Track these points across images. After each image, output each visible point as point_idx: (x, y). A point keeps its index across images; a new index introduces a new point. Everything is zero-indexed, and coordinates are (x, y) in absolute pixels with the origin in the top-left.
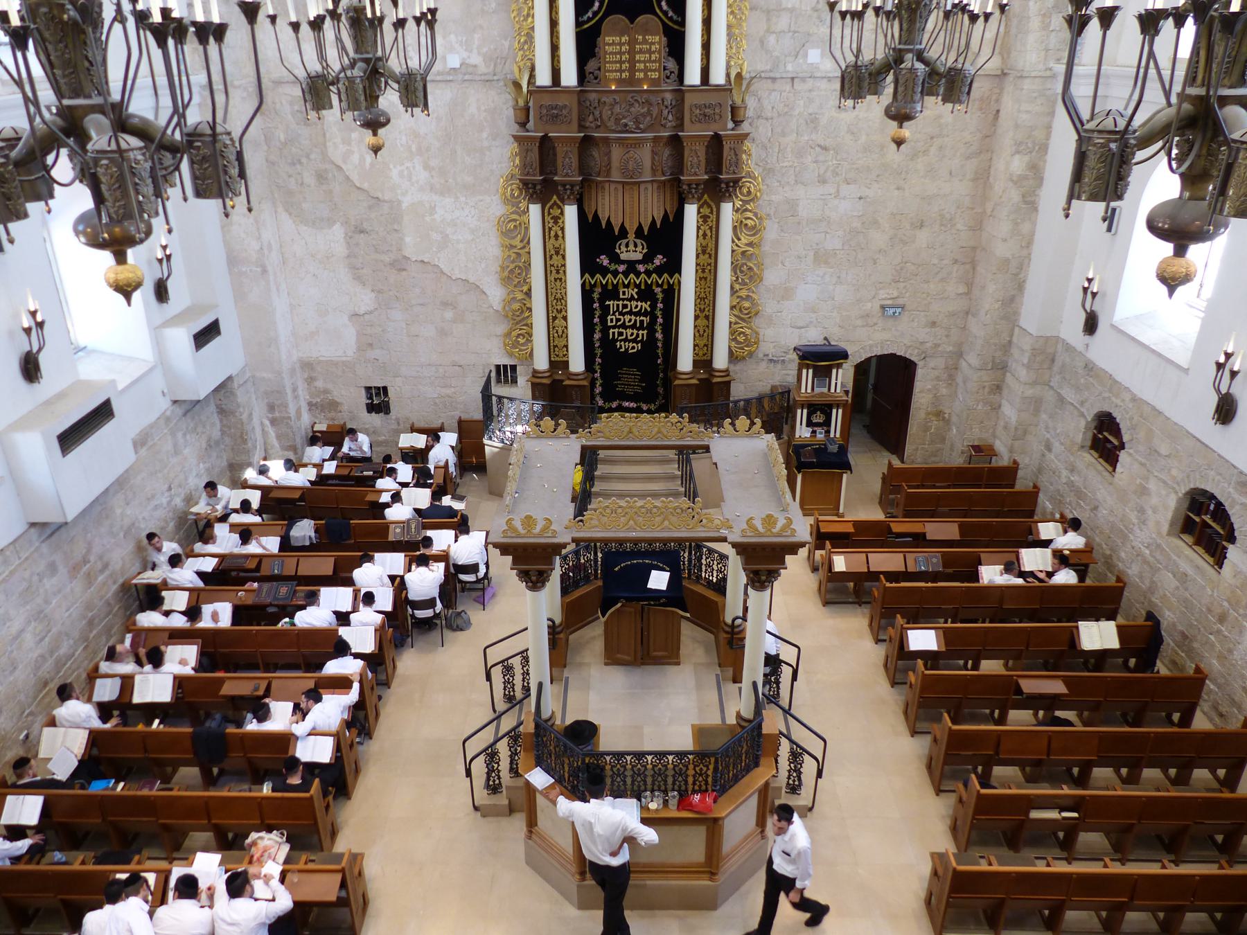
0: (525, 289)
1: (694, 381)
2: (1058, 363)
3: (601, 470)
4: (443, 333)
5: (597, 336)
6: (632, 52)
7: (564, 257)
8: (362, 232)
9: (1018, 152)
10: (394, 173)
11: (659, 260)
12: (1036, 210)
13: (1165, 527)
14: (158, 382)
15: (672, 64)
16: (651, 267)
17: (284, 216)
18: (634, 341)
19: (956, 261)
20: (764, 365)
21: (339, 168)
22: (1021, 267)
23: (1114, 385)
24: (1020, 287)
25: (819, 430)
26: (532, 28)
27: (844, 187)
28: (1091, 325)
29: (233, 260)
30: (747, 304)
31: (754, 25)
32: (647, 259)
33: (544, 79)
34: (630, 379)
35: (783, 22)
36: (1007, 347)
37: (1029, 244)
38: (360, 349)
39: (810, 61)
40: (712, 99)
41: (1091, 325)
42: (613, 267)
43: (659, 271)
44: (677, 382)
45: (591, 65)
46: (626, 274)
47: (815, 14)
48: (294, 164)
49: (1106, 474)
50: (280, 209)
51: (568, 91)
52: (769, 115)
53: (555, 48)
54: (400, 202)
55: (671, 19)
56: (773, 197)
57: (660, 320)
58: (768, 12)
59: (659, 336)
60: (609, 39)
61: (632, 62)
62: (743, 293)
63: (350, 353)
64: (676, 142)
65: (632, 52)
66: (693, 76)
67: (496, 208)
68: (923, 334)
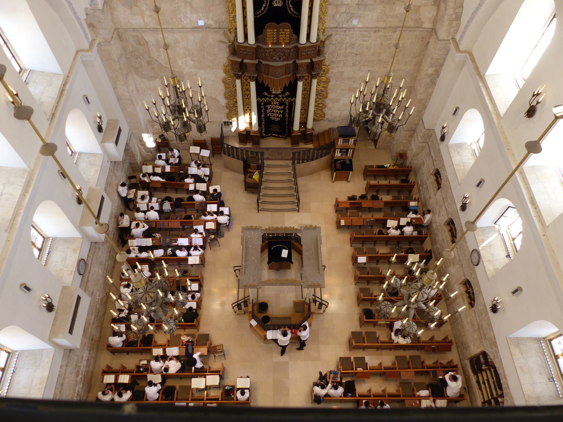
0: (235, 100)
1: (300, 134)
3: (266, 170)
5: (263, 116)
6: (278, 35)
7: (250, 91)
9: (431, 67)
10: (180, 62)
11: (287, 94)
12: (435, 84)
13: (443, 223)
14: (106, 158)
15: (295, 36)
16: (284, 96)
17: (135, 76)
18: (277, 117)
20: (326, 122)
21: (156, 60)
22: (426, 102)
23: (443, 165)
24: (425, 108)
25: (344, 154)
26: (235, 16)
29: (119, 99)
30: (321, 105)
31: (331, 10)
32: (282, 93)
33: (241, 39)
34: (276, 128)
35: (343, 9)
36: (417, 124)
39: (353, 23)
41: (443, 138)
42: (269, 96)
43: (287, 97)
44: (293, 134)
45: (261, 36)
46: (274, 98)
47: (357, 6)
48: (137, 58)
49: (435, 189)
50: (134, 74)
52: (334, 42)
53: (245, 26)
54: (182, 72)
55: (295, 14)
56: (334, 71)
57: (287, 111)
58: (337, 6)
59: (287, 115)
60: (269, 30)
62: (320, 102)
64: (295, 65)
65: (278, 35)
66: (303, 39)
67: (222, 75)
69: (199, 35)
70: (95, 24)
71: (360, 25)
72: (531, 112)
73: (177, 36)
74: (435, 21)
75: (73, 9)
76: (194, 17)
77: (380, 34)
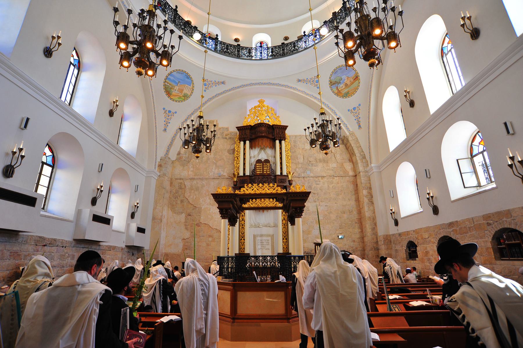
2: (392, 241)
4: (208, 245)
6: (263, 167)
8: (190, 215)
10: (201, 200)
14: (124, 238)
19: (356, 223)
24: (375, 224)
27: (321, 203)
28: (396, 223)
29: (154, 219)
33: (241, 174)
35: (300, 166)
37: (374, 213)
38: (183, 250)
40: (284, 178)
50: (169, 209)
51: (247, 176)
61: (263, 169)
63: (180, 251)
65: (263, 167)
68: (352, 244)
69: (217, 181)
70: (163, 164)
71: (312, 175)
72: (412, 104)
73: (204, 182)
74: (355, 169)
75: (156, 156)
76: (216, 171)
77: (325, 179)
